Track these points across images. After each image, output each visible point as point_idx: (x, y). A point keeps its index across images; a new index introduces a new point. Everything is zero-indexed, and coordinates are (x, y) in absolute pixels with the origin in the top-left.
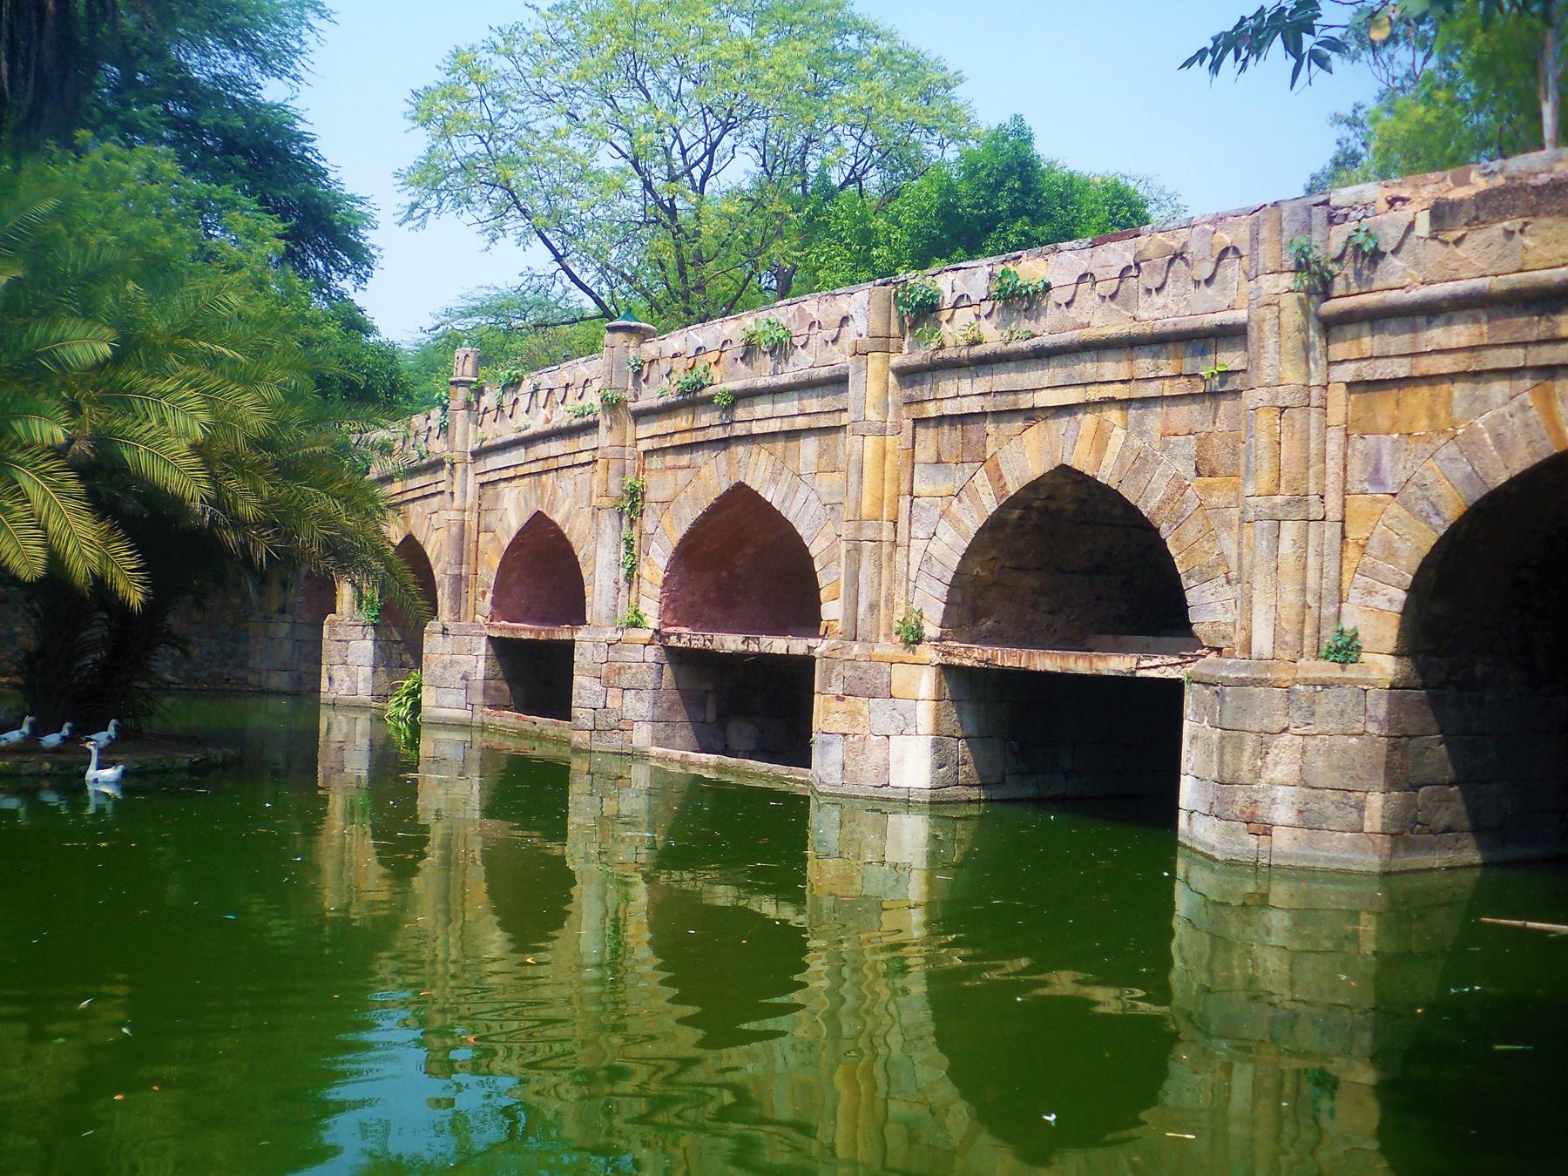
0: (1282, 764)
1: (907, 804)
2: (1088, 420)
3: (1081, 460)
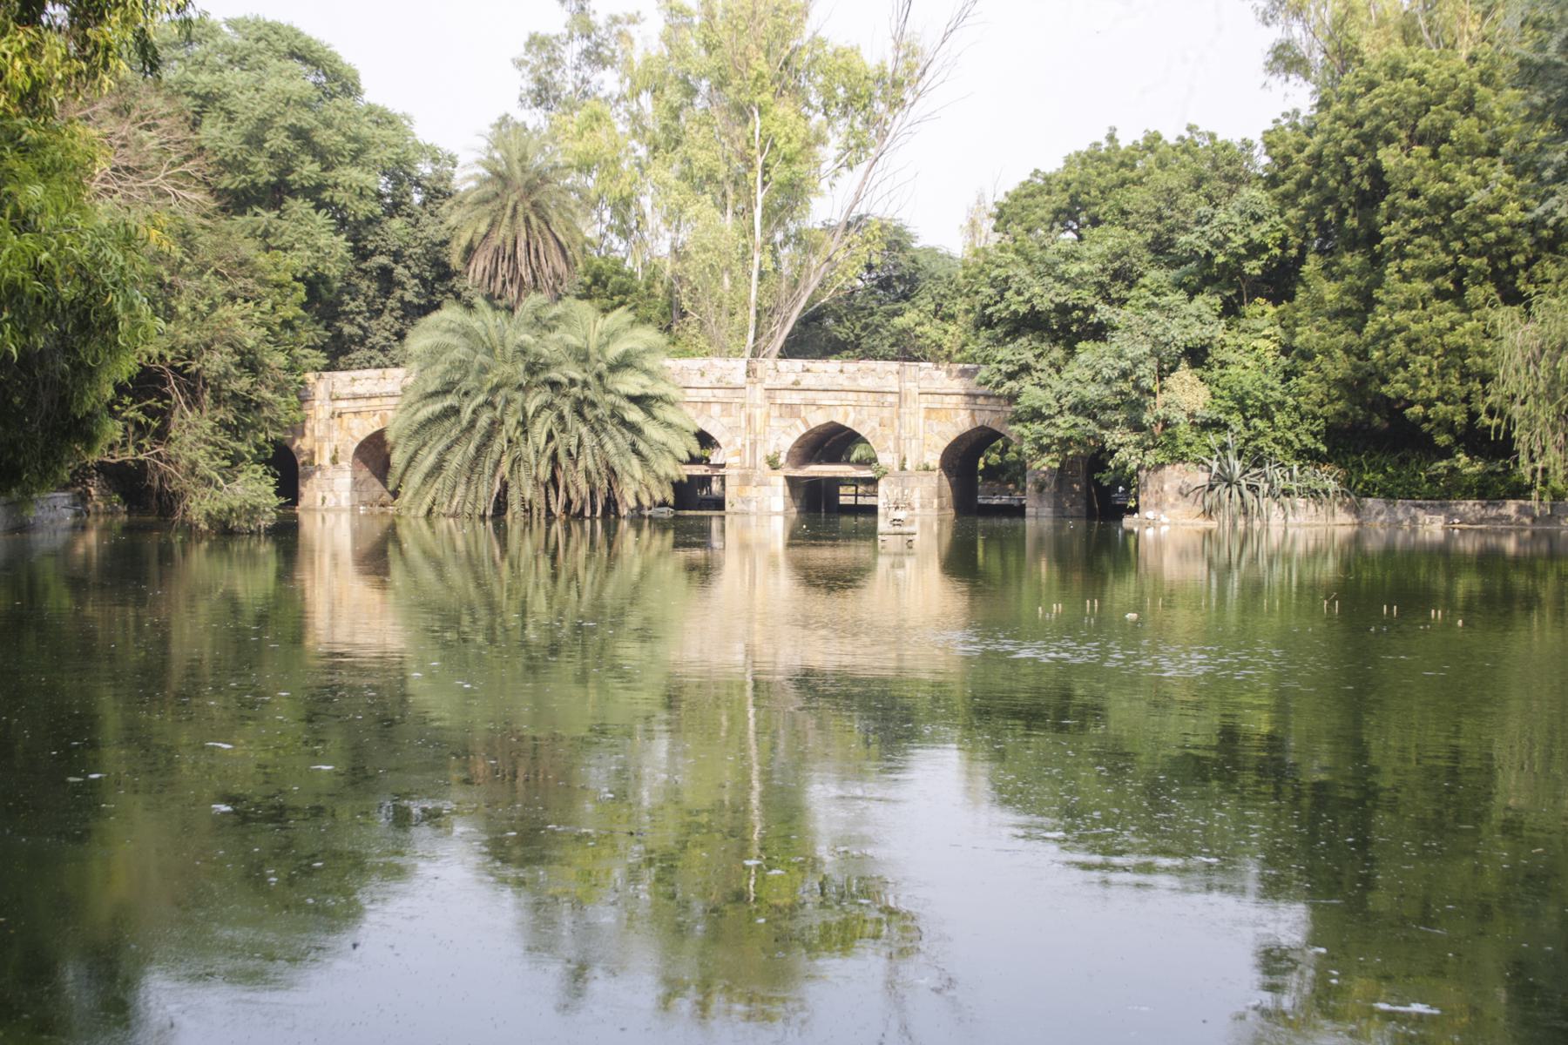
0: (917, 494)
1: (777, 514)
2: (841, 410)
3: (840, 420)
